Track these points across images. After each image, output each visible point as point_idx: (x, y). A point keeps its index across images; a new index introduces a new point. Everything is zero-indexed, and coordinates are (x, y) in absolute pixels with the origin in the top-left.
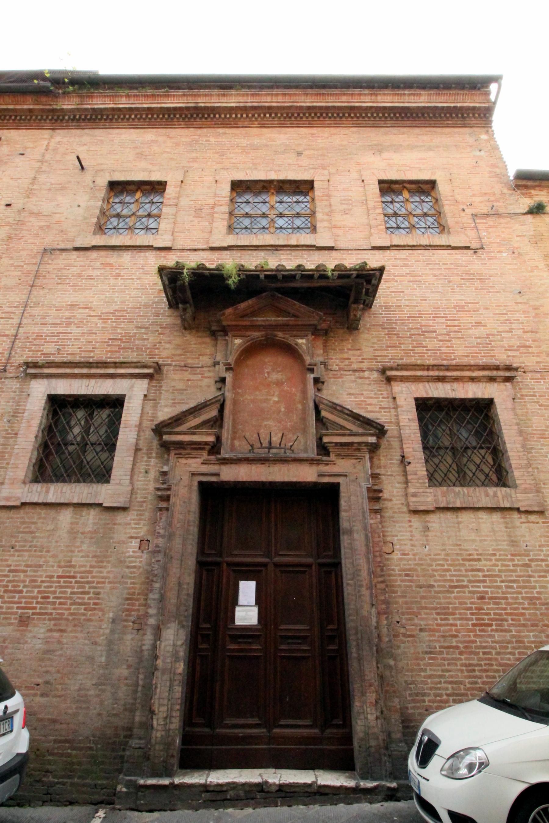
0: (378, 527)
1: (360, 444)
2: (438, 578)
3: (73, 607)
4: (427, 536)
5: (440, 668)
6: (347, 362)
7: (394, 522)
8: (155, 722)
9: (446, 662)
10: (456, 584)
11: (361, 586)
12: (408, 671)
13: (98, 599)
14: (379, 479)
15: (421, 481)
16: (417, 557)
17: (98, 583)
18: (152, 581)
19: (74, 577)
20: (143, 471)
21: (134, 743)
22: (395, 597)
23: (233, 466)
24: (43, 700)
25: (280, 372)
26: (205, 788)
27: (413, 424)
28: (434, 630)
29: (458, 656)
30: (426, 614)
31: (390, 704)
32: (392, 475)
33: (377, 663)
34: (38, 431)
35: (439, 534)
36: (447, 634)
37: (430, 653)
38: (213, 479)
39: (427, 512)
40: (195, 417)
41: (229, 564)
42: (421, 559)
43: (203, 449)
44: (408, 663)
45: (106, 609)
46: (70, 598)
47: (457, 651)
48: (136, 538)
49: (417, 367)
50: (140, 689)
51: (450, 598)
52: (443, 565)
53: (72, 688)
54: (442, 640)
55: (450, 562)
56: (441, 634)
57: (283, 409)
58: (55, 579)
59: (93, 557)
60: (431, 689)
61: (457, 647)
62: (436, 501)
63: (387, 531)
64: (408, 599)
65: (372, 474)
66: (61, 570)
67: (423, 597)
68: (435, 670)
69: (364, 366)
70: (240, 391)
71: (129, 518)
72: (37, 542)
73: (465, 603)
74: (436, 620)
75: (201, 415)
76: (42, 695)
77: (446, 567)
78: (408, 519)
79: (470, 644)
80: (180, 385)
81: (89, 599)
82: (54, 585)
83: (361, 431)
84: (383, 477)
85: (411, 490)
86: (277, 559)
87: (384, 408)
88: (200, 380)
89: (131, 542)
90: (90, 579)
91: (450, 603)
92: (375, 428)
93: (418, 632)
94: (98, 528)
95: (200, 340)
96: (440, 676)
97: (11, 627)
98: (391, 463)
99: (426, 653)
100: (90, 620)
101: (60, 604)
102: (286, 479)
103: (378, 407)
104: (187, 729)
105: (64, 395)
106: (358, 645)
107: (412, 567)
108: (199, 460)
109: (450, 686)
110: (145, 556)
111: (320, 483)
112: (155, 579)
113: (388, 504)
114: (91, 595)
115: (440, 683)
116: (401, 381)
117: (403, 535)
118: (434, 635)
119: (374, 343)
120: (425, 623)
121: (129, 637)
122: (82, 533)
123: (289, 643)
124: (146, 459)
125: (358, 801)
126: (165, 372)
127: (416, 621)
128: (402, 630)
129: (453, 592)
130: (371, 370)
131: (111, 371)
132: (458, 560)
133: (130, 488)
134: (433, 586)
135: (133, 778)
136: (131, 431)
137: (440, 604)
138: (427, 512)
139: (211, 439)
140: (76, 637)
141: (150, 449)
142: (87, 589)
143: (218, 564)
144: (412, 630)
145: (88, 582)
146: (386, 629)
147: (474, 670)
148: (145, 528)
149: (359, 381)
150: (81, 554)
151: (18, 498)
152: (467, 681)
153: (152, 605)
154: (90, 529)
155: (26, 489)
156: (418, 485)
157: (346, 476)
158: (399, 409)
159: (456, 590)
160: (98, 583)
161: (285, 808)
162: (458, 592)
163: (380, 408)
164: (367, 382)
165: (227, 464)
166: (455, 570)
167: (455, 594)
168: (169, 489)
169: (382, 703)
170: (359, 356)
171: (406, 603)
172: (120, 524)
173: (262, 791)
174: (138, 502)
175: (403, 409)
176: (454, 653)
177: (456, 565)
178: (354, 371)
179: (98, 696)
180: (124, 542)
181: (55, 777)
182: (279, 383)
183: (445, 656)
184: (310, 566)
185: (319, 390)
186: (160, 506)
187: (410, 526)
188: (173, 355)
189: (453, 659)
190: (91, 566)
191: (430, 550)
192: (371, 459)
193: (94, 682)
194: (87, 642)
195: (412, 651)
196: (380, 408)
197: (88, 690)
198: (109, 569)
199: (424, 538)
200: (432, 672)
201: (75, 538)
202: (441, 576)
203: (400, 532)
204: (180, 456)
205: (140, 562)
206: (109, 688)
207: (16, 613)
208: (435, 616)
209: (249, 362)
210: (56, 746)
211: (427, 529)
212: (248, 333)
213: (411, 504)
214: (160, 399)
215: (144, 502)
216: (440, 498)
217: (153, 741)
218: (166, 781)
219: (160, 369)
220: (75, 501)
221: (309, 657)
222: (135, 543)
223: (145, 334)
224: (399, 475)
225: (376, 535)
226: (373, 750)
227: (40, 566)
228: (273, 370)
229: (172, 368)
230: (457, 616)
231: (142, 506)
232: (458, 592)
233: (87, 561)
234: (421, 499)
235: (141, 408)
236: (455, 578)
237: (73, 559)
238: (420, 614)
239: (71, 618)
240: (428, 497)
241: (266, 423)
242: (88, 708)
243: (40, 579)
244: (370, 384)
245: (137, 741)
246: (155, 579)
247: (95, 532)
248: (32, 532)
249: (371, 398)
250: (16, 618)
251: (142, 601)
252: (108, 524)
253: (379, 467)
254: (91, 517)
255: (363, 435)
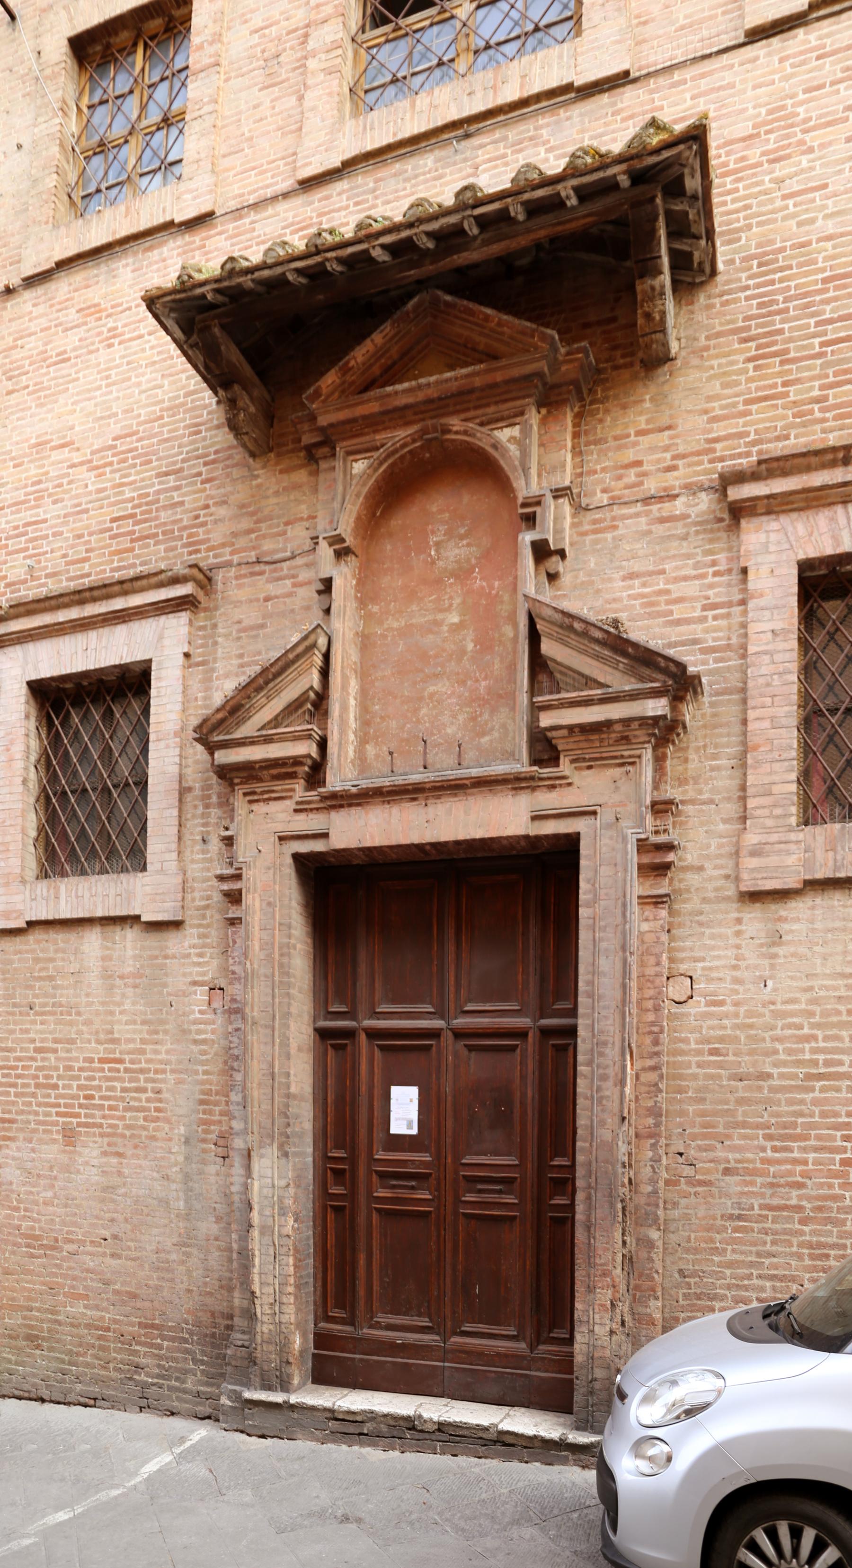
0: (658, 941)
1: (626, 722)
2: (782, 1057)
3: (128, 1114)
4: (774, 956)
5: (754, 1249)
6: (631, 476)
7: (701, 924)
8: (258, 1311)
9: (769, 1239)
10: (822, 1070)
11: (604, 1078)
12: (687, 1251)
13: (160, 1101)
14: (679, 813)
15: (778, 811)
16: (742, 1010)
17: (156, 1072)
18: (232, 1068)
19: (120, 1061)
20: (198, 838)
21: (238, 1337)
22: (680, 1101)
23: (354, 811)
24: (115, 1262)
25: (462, 537)
26: (332, 1415)
27: (782, 646)
28: (754, 1172)
29: (798, 1226)
30: (745, 1137)
31: (641, 1310)
32: (711, 801)
33: (623, 1234)
34: (26, 769)
35: (802, 950)
36: (782, 1181)
37: (740, 1218)
38: (318, 846)
39: (782, 895)
40: (269, 698)
41: (373, 1034)
42: (750, 1014)
43: (292, 776)
44: (689, 1237)
45: (174, 1119)
46: (122, 1099)
47: (797, 1216)
48: (202, 984)
49: (814, 460)
50: (235, 1256)
51: (802, 1102)
52: (801, 1027)
53: (149, 1248)
54: (769, 1192)
55: (817, 1019)
56: (769, 1180)
57: (470, 646)
58: (96, 1065)
59: (144, 1022)
60: (729, 1287)
61: (799, 1208)
62: (807, 864)
63: (682, 949)
64: (708, 1107)
65: (654, 804)
66: (101, 1048)
67: (741, 1101)
68: (742, 1253)
69: (674, 480)
70: (375, 609)
71: (186, 944)
72: (61, 996)
73: (836, 1115)
74: (764, 1149)
75: (279, 692)
76: (113, 1255)
77: (806, 1031)
78: (736, 915)
79: (829, 1203)
80: (250, 616)
81: (148, 1100)
82: (98, 1075)
83: (630, 685)
84: (689, 809)
85: (752, 838)
86: (460, 1022)
87: (714, 606)
88: (290, 595)
89: (195, 993)
90: (143, 1065)
91: (801, 1114)
92: (665, 671)
93: (719, 1176)
94: (142, 966)
95: (287, 480)
96: (751, 1264)
97: (55, 1147)
98: (712, 769)
99: (731, 1217)
100: (153, 1138)
101: (111, 1108)
102: (462, 835)
103: (699, 605)
104: (322, 1325)
105: (52, 679)
106: (589, 1198)
107: (729, 1032)
108: (290, 804)
109: (768, 1284)
110: (220, 1020)
111: (538, 838)
112: (235, 1064)
113: (693, 879)
114: (150, 1094)
115: (749, 1277)
116: (769, 512)
117: (719, 957)
118: (752, 1183)
119: (709, 399)
120: (738, 1156)
121: (212, 1169)
122: (121, 977)
123: (481, 1191)
124: (200, 810)
125: (564, 1462)
126: (220, 586)
127: (720, 1154)
128: (688, 1171)
129: (813, 1090)
130: (692, 489)
131: (118, 604)
132: (839, 1013)
133: (179, 879)
134: (769, 1076)
135: (237, 1388)
136: (167, 747)
137: (778, 1115)
138: (782, 895)
139: (307, 748)
140: (140, 1166)
141: (206, 787)
142: (142, 1084)
143: (350, 1034)
144: (708, 1172)
145: (142, 1071)
146: (649, 1169)
147: (827, 1256)
148: (215, 963)
149: (660, 530)
150: (125, 1018)
151: (20, 913)
152: (807, 1276)
153: (236, 1114)
154: (131, 969)
155: (27, 893)
156: (769, 823)
157: (594, 813)
158: (751, 605)
159: (818, 1084)
160: (156, 1072)
161: (447, 1459)
162: (823, 1090)
163: (704, 608)
164: (679, 529)
165: (342, 806)
166: (826, 1039)
167: (817, 1094)
168: (238, 877)
169: (624, 1307)
170: (666, 449)
171: (703, 1114)
172: (174, 957)
173: (413, 1428)
174: (198, 909)
175: (762, 602)
176: (789, 1219)
177: (833, 1025)
178: (647, 500)
179: (183, 1262)
180: (184, 994)
181: (148, 1375)
182: (462, 573)
183: (768, 1225)
184: (521, 1034)
185: (552, 577)
186: (230, 915)
187: (738, 934)
188: (234, 535)
189: (785, 1232)
190: (143, 1041)
191: (775, 990)
192: (659, 760)
193: (175, 1240)
194: (155, 1174)
195: (701, 1213)
196: (704, 608)
197: (169, 1252)
198: (169, 1046)
199: (766, 962)
200: (736, 1257)
201: (112, 987)
202: (789, 1052)
203: (713, 948)
204: (253, 798)
205: (213, 1032)
206: (194, 1251)
207: (56, 1124)
208: (762, 1141)
209: (397, 522)
210: (142, 1332)
211: (777, 938)
212: (379, 437)
213: (745, 876)
214: (215, 660)
215: (207, 907)
216: (820, 854)
217: (259, 1339)
218: (278, 1397)
219: (209, 579)
220: (99, 913)
221: (514, 1217)
222: (201, 994)
223: (177, 488)
224: (729, 799)
225: (652, 960)
226: (597, 1385)
227: (72, 1041)
228: (449, 534)
229: (233, 572)
230: (812, 1142)
231: (204, 917)
232: (823, 1090)
233: (135, 1031)
234: (772, 861)
235: (180, 689)
236: (821, 1057)
237: (116, 1027)
238: (729, 1137)
239: (128, 1133)
240: (789, 853)
241: (432, 689)
242: (172, 1280)
243: (76, 1065)
244: (685, 538)
245: (239, 1336)
246: (235, 1064)
247: (138, 975)
248: (51, 978)
249: (685, 578)
250: (58, 1132)
251: (223, 1107)
252: (156, 957)
253: (682, 781)
254: (129, 944)
255: (633, 696)
